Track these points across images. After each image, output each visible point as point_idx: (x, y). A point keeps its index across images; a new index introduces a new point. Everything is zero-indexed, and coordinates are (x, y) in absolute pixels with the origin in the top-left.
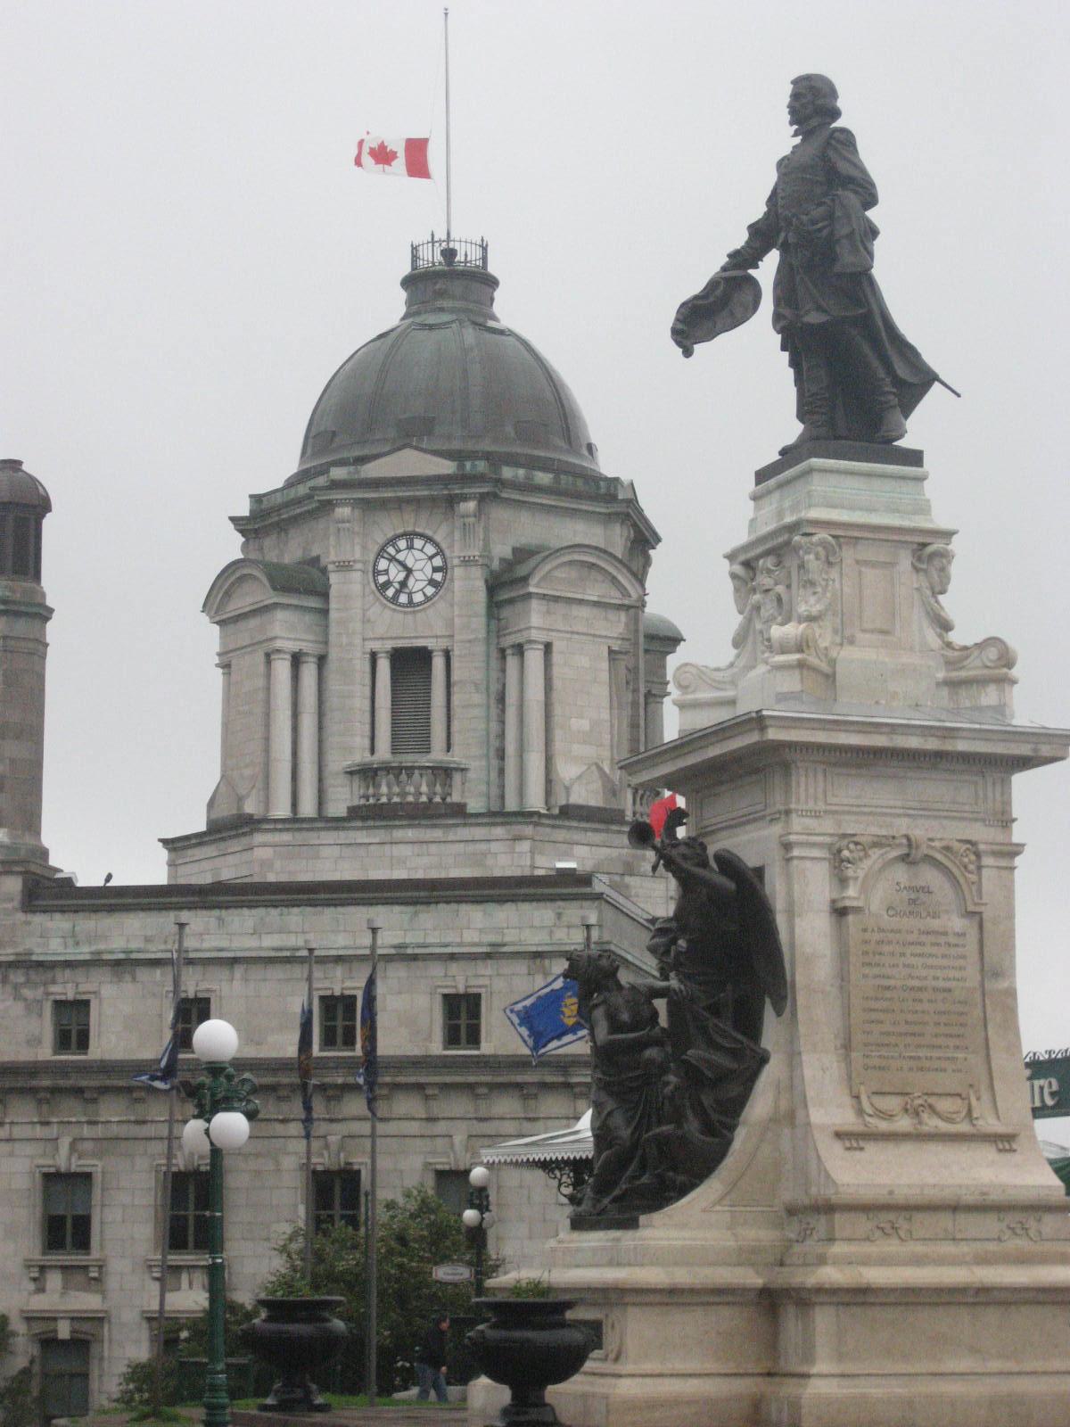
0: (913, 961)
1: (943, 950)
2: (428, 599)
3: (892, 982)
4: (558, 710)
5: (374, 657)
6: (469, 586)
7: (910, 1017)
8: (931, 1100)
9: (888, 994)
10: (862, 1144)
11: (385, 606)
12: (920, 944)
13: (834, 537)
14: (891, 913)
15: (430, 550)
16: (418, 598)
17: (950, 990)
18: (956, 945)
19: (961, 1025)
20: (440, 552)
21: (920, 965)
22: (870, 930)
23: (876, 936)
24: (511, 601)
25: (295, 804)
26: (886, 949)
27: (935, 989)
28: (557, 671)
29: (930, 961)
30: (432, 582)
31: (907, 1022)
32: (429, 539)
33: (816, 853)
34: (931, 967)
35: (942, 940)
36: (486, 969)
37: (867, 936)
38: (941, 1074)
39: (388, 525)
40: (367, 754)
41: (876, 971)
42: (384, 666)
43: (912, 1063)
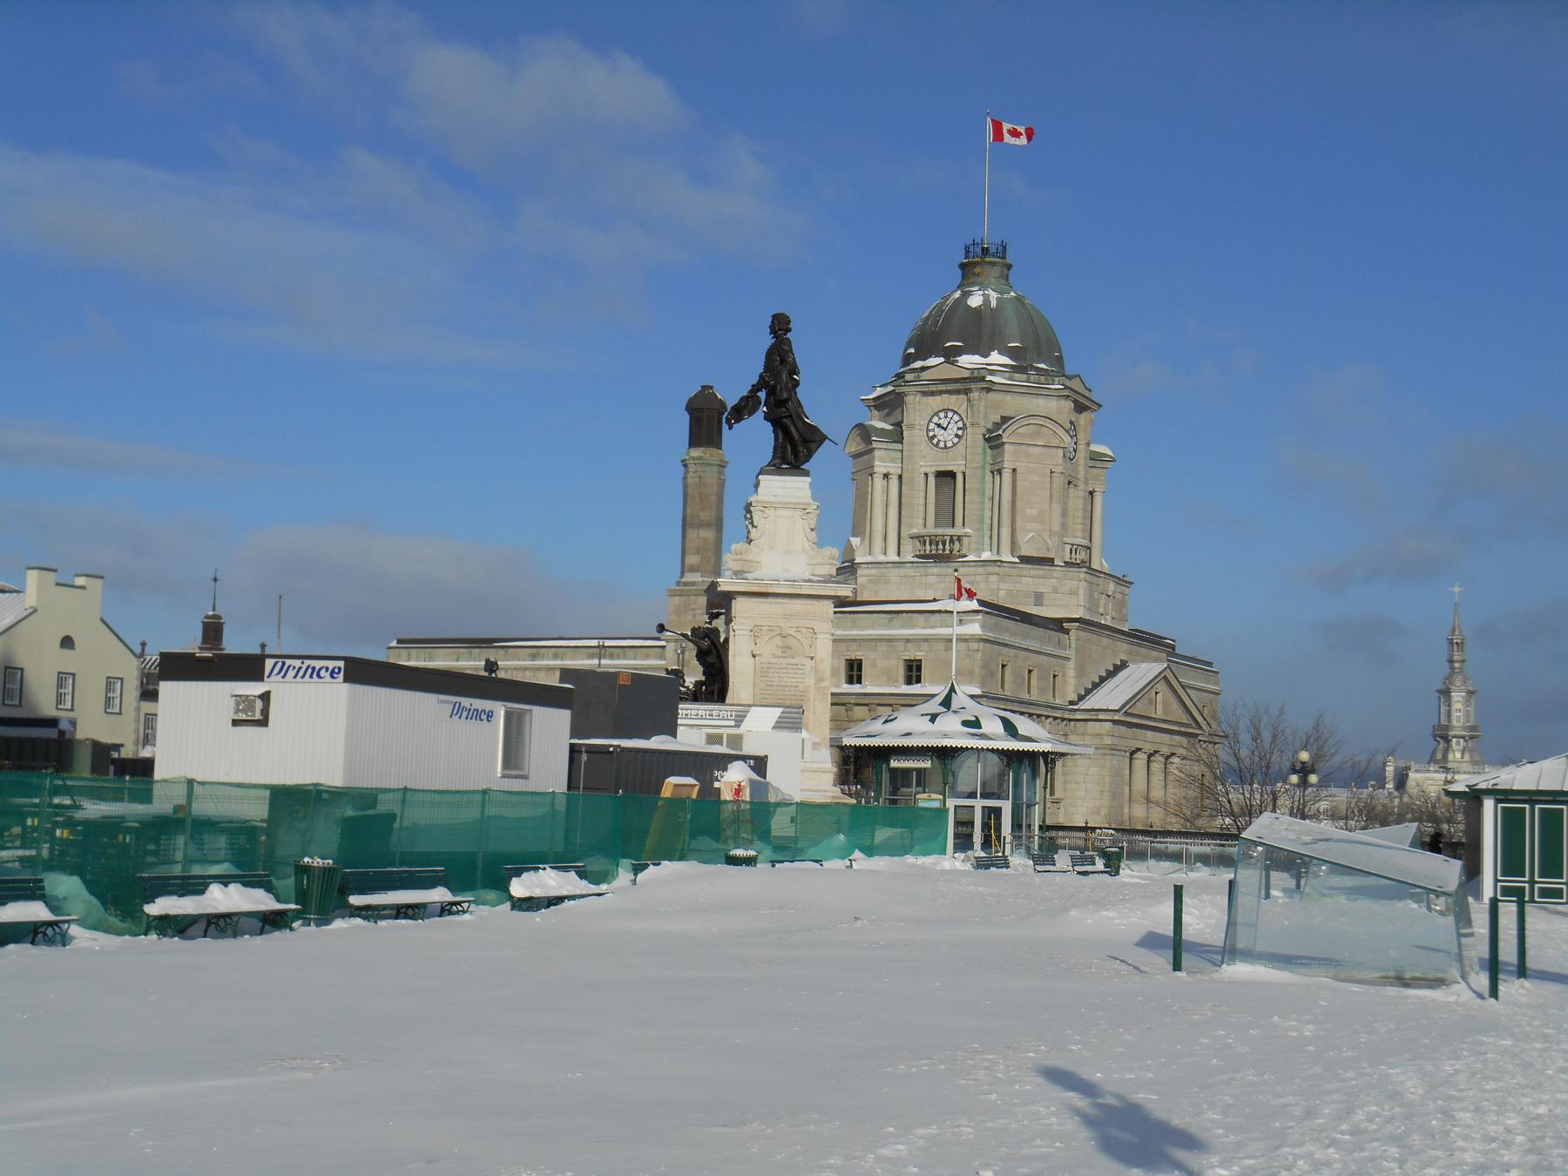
1: (796, 671)
2: (955, 445)
3: (773, 684)
4: (1019, 504)
6: (976, 436)
7: (779, 697)
9: (771, 688)
11: (932, 449)
15: (956, 418)
16: (949, 444)
17: (797, 687)
23: (768, 666)
26: (770, 670)
27: (791, 686)
28: (1019, 484)
29: (790, 675)
30: (957, 436)
32: (955, 412)
35: (795, 667)
36: (925, 646)
37: (763, 665)
40: (921, 527)
41: (766, 679)
42: (932, 480)
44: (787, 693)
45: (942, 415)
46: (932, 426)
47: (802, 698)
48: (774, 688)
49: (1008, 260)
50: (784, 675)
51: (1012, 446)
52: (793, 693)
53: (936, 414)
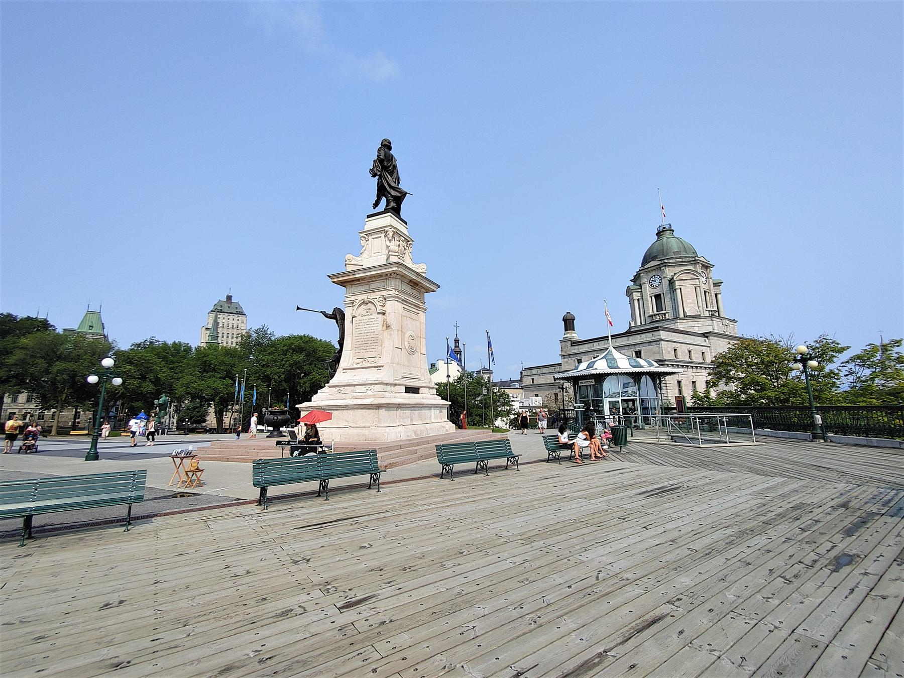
1: (374, 322)
5: (651, 297)
13: (366, 235)
15: (658, 277)
20: (660, 277)
23: (359, 322)
24: (673, 282)
25: (641, 323)
26: (361, 324)
29: (370, 326)
30: (659, 282)
33: (675, 315)
35: (373, 320)
37: (357, 322)
39: (651, 274)
41: (359, 330)
42: (653, 298)
44: (369, 337)
45: (653, 277)
46: (651, 281)
47: (377, 339)
48: (362, 335)
49: (672, 228)
51: (678, 282)
53: (652, 277)
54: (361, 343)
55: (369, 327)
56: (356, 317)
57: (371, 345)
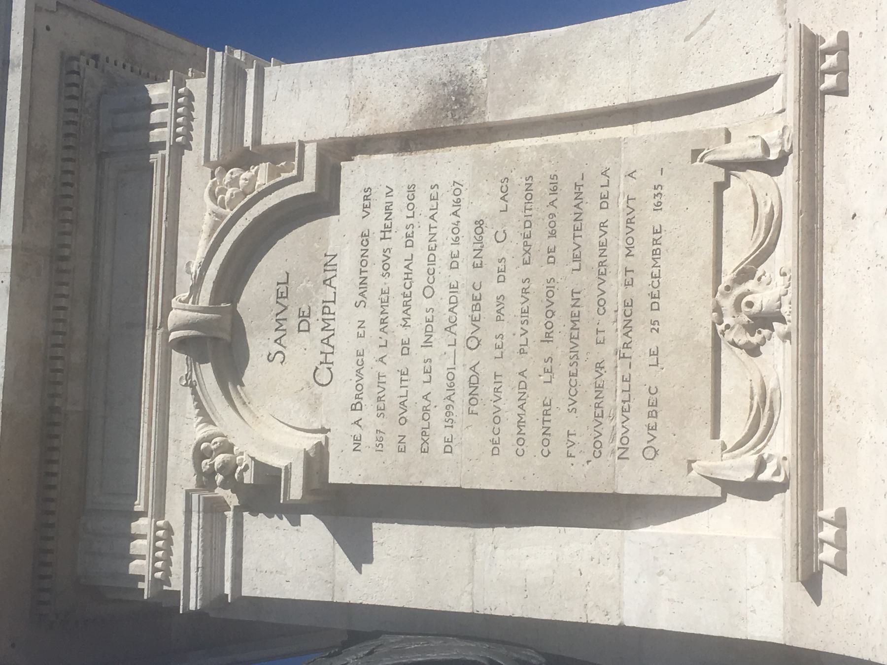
0: (417, 318)
3: (462, 375)
7: (537, 330)
8: (730, 265)
9: (486, 390)
10: (827, 512)
12: (384, 303)
14: (324, 377)
17: (479, 224)
18: (388, 210)
19: (554, 191)
21: (428, 303)
22: (356, 430)
23: (369, 413)
29: (420, 280)
31: (548, 338)
34: (431, 273)
35: (376, 249)
37: (369, 439)
38: (666, 241)
41: (437, 417)
43: (640, 329)
44: (512, 288)
47: (541, 189)
48: (486, 371)
50: (419, 304)
52: (515, 243)
54: (561, 380)
55: (429, 291)
56: (322, 450)
57: (591, 258)
